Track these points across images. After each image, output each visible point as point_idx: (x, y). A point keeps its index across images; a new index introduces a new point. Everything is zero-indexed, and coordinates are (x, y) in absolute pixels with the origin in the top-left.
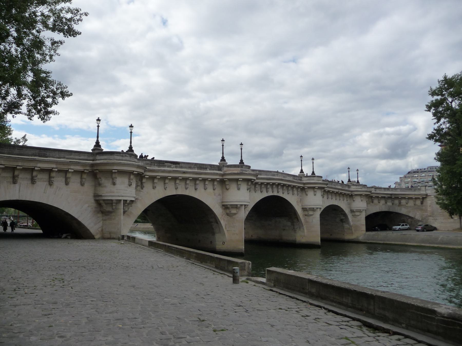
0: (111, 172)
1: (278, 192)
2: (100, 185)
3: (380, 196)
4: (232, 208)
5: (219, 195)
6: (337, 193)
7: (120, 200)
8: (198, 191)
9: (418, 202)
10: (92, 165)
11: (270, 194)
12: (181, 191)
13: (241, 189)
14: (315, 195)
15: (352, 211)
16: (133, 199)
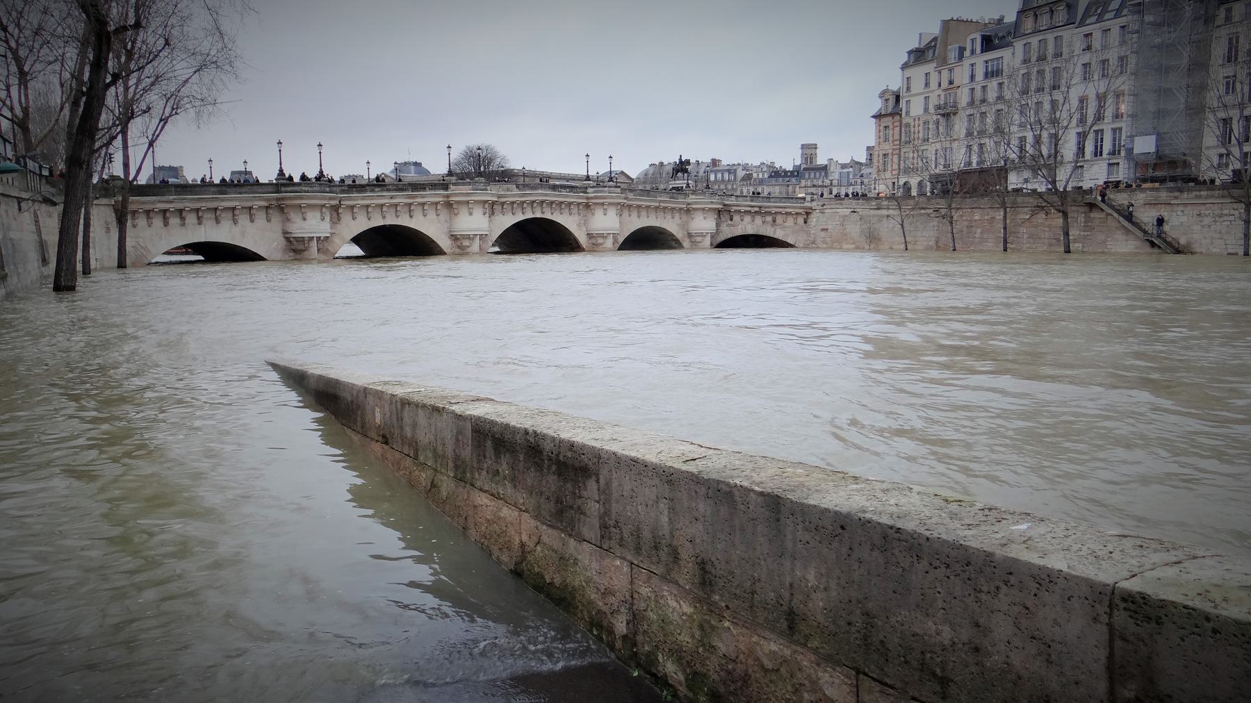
0: (300, 206)
1: (543, 213)
2: (288, 220)
3: (743, 209)
4: (463, 238)
5: (446, 221)
6: (657, 208)
7: (313, 237)
8: (414, 219)
9: (801, 220)
10: (278, 199)
11: (529, 215)
12: (391, 220)
13: (474, 214)
14: (605, 214)
15: (690, 235)
16: (329, 235)
